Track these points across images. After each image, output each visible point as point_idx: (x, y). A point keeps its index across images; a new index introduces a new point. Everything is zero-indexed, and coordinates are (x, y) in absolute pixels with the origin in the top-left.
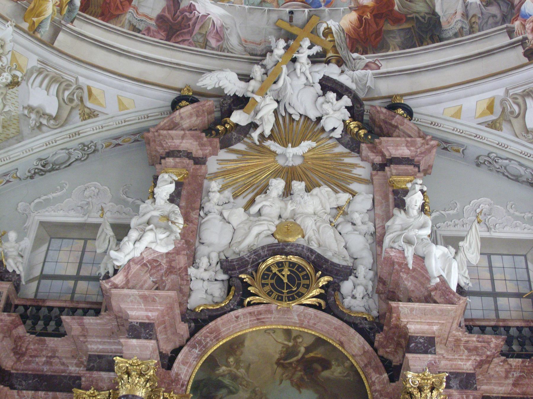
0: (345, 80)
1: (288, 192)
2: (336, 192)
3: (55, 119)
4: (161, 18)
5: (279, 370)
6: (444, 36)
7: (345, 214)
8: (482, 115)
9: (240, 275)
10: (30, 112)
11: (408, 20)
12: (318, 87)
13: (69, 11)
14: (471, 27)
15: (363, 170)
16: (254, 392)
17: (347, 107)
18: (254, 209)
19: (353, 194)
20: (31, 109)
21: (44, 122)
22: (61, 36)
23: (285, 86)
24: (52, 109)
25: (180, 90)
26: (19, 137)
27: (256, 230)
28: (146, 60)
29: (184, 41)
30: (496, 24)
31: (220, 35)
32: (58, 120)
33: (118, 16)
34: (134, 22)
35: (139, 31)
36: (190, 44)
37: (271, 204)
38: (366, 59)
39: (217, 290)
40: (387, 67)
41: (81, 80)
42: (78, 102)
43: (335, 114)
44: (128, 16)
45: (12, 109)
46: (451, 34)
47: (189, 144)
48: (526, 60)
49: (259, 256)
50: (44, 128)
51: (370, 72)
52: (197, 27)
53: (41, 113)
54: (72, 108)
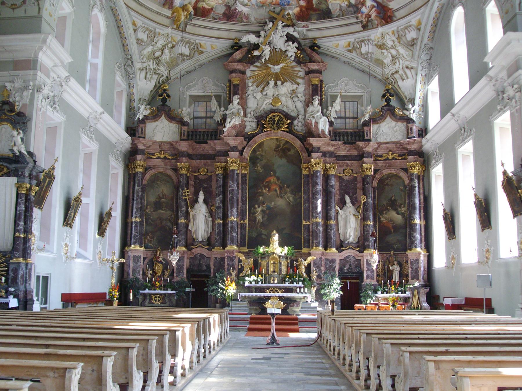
2: (293, 84)
3: (189, 56)
11: (319, 10)
12: (285, 38)
15: (302, 74)
17: (296, 47)
21: (185, 58)
23: (273, 38)
26: (177, 65)
28: (220, 29)
30: (352, 14)
31: (247, 17)
32: (190, 57)
36: (236, 22)
42: (197, 49)
43: (292, 50)
46: (335, 16)
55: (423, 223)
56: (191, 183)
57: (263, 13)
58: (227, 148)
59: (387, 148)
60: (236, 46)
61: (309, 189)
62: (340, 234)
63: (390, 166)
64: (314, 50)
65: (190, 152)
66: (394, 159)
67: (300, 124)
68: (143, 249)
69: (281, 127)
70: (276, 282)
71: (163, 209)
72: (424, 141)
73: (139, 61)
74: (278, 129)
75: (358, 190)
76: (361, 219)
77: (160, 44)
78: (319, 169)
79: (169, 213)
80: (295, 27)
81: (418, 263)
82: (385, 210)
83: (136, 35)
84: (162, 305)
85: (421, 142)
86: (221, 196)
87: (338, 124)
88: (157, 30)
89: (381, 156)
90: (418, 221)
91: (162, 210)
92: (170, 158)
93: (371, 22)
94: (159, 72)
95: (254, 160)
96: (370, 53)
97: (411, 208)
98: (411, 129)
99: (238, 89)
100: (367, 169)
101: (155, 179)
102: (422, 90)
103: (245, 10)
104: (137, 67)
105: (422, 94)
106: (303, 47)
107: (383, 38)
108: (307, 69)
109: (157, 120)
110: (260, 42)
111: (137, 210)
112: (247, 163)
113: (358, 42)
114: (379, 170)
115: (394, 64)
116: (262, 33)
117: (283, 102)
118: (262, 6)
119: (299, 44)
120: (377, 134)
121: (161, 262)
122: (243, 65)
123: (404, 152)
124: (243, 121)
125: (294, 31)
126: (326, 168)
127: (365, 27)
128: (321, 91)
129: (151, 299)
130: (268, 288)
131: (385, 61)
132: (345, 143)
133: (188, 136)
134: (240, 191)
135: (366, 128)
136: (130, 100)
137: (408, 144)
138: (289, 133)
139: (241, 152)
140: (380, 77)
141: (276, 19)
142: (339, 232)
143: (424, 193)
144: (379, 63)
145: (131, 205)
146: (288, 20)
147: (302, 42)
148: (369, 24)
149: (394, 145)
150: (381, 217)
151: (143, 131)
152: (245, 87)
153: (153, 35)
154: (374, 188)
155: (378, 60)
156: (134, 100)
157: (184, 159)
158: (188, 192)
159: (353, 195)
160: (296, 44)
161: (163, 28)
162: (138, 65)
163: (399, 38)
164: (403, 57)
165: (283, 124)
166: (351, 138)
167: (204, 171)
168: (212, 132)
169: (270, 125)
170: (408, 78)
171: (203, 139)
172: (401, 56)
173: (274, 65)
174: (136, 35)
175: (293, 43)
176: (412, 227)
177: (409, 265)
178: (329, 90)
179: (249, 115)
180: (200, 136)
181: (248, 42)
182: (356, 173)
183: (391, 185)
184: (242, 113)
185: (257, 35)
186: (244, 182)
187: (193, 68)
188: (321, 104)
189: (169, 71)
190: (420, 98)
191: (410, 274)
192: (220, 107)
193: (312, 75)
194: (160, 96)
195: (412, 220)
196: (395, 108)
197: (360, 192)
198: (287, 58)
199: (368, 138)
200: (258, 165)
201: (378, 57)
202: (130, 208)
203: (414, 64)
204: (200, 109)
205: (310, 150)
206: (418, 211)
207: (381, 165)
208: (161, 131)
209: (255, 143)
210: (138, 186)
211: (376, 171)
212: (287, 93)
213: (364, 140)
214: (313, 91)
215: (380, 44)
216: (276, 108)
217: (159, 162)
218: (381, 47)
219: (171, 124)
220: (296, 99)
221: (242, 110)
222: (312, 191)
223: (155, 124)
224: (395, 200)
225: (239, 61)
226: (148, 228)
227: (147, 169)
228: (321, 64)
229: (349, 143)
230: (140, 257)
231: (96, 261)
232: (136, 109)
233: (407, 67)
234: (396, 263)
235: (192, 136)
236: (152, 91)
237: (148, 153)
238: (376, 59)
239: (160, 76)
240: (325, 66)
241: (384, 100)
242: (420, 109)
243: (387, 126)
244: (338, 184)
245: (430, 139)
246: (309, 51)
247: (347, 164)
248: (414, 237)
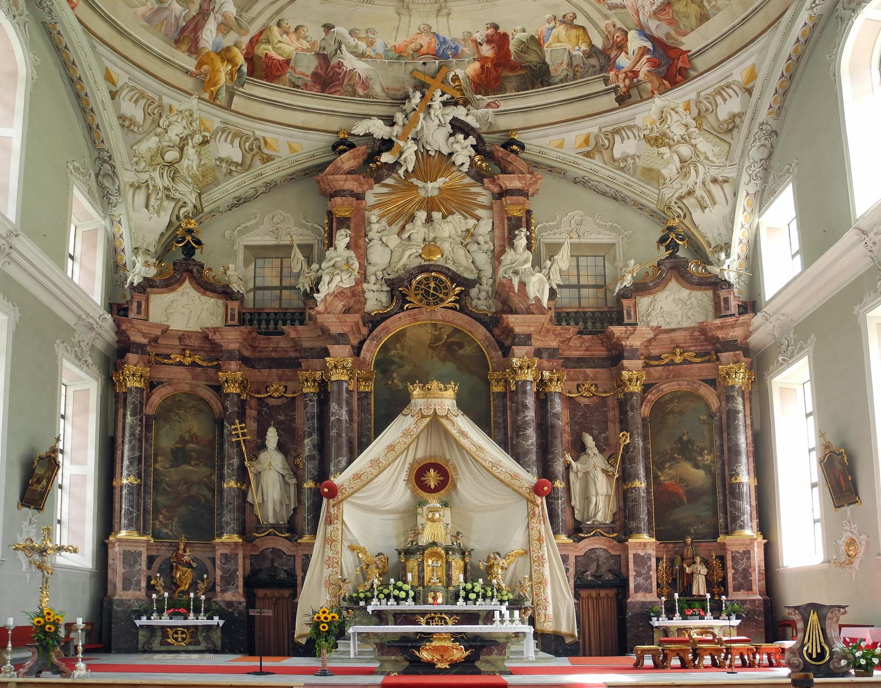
17: (472, 146)
37: (418, 230)
42: (257, 151)
47: (350, 184)
107: (663, 120)
110: (395, 134)
115: (686, 175)
118: (400, 57)
119: (479, 138)
144: (652, 176)
160: (472, 140)
164: (707, 158)
170: (714, 203)
172: (702, 157)
181: (369, 135)
198: (454, 169)
201: (649, 164)
203: (730, 173)
215: (654, 135)
218: (658, 141)
233: (715, 181)
246: (501, 152)
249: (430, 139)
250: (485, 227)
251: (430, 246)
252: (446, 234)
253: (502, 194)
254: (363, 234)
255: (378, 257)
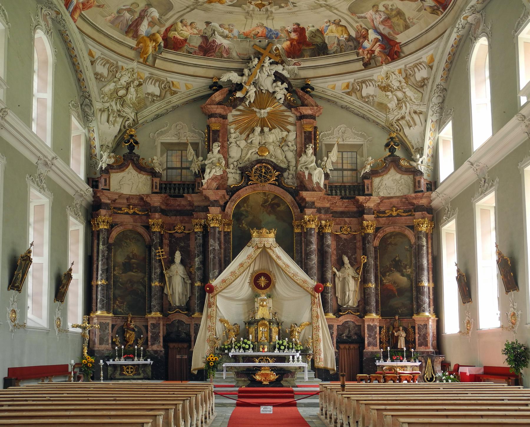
0: (285, 73)
1: (262, 131)
4: (200, 47)
5: (262, 208)
6: (329, 52)
7: (285, 141)
8: (344, 89)
9: (245, 172)
10: (148, 96)
11: (313, 45)
12: (273, 77)
13: (159, 49)
14: (341, 50)
15: (292, 119)
16: (254, 216)
17: (286, 88)
18: (249, 141)
19: (289, 131)
20: (148, 94)
21: (155, 99)
22: (157, 61)
24: (157, 92)
25: (212, 78)
26: (146, 107)
27: (250, 152)
28: (196, 66)
29: (211, 55)
31: (228, 51)
32: (161, 97)
33: (181, 48)
34: (189, 49)
35: (191, 53)
37: (256, 138)
38: (294, 61)
39: (238, 177)
40: (303, 65)
41: (168, 79)
42: (168, 88)
44: (185, 47)
45: (141, 95)
47: (219, 110)
48: (363, 68)
49: (252, 164)
50: (155, 101)
51: (296, 67)
52: (217, 49)
53: (153, 95)
54: (166, 91)
55: (432, 285)
56: (166, 241)
57: (246, 47)
58: (206, 204)
59: (391, 203)
60: (216, 86)
61: (301, 249)
62: (337, 298)
63: (394, 223)
64: (307, 92)
65: (163, 207)
66: (398, 215)
67: (291, 176)
68: (111, 315)
69: (269, 180)
70: (266, 350)
71: (134, 270)
72: (434, 195)
73: (99, 100)
74: (266, 181)
75: (358, 250)
76: (360, 282)
77: (124, 80)
78: (313, 226)
79: (140, 275)
80: (284, 64)
81: (426, 328)
82: (388, 272)
83: (94, 69)
84: (136, 377)
85: (429, 197)
86: (201, 256)
87: (335, 177)
88: (120, 64)
89: (384, 212)
90: (426, 283)
91: (133, 271)
92: (140, 213)
93: (374, 58)
94: (125, 114)
95: (238, 216)
96: (372, 96)
97: (419, 269)
98: (419, 182)
99: (219, 136)
100: (367, 226)
101: (123, 237)
102: (432, 139)
103: (225, 43)
104: (97, 107)
105: (432, 143)
106: (294, 88)
107: (388, 78)
108: (298, 114)
109: (123, 171)
110: (244, 81)
111: (103, 272)
112: (230, 220)
113: (358, 83)
114: (381, 228)
115: (400, 108)
116: (246, 71)
117: (271, 152)
118: (246, 38)
119: (289, 84)
120: (379, 188)
121: (134, 330)
122: (224, 108)
123: (411, 207)
124: (224, 172)
125: (283, 70)
126: (321, 226)
127: (367, 65)
128: (315, 139)
129: (122, 370)
130: (257, 357)
131: (389, 105)
132: (342, 198)
133: (161, 188)
134: (223, 251)
135: (366, 182)
136: (89, 147)
137: (415, 198)
138: (279, 186)
139: (223, 208)
140: (383, 124)
141: (262, 54)
142: (337, 295)
143: (432, 252)
144: (382, 107)
145: (95, 266)
146: (276, 55)
147: (293, 82)
148: (372, 61)
149: (398, 200)
150: (383, 279)
151: (107, 182)
152: (227, 133)
153: (115, 71)
154: (375, 248)
155: (382, 104)
156: (95, 147)
157: (157, 215)
158: (162, 252)
159: (352, 255)
160: (285, 85)
161: (127, 62)
162: (98, 105)
163: (407, 78)
164: (411, 100)
165: (271, 176)
166: (350, 192)
167: (180, 228)
168: (188, 185)
169: (257, 177)
170: (415, 124)
171: (179, 193)
172: (408, 99)
173: (260, 109)
174: (94, 69)
175: (282, 84)
176: (419, 290)
177: (417, 331)
178: (324, 138)
179: (232, 166)
180: (175, 189)
181: (230, 81)
182: (355, 232)
183: (395, 244)
184: (224, 162)
185: (240, 73)
186: (227, 241)
187: (165, 111)
188: (315, 153)
189: (137, 114)
190: (429, 147)
191: (417, 340)
192: (198, 157)
193: (304, 121)
194: (126, 143)
195: (419, 282)
196: (400, 159)
197: (359, 252)
198: (276, 101)
199: (369, 192)
200: (243, 222)
201: (381, 100)
202: (95, 270)
203: (423, 109)
204: (174, 159)
205: (302, 205)
206: (426, 273)
207: (383, 222)
208: (129, 183)
209: (239, 198)
210: (103, 245)
211: (377, 229)
212: (275, 142)
213: (364, 195)
214: (305, 139)
215: (383, 85)
216: (263, 158)
217: (127, 219)
218: (386, 88)
219: (140, 175)
220: (286, 148)
221: (223, 159)
222: (306, 250)
223: (120, 175)
224: (400, 261)
225: (219, 103)
226: (118, 292)
227: (112, 226)
228: (315, 108)
229: (348, 198)
230: (108, 324)
231: (55, 330)
232: (98, 157)
233: (415, 112)
234: (401, 328)
235: (165, 188)
236: (116, 136)
237: (114, 208)
238: (378, 102)
239: (126, 119)
240: (320, 111)
241: (387, 150)
242: (429, 160)
243: (390, 179)
244: (334, 243)
245: (441, 193)
246: (301, 93)
247: (345, 221)
248: (422, 301)
249: (263, 84)
250: (292, 136)
251: (263, 147)
252: (271, 141)
253: (301, 117)
254: (226, 139)
255: (235, 153)
